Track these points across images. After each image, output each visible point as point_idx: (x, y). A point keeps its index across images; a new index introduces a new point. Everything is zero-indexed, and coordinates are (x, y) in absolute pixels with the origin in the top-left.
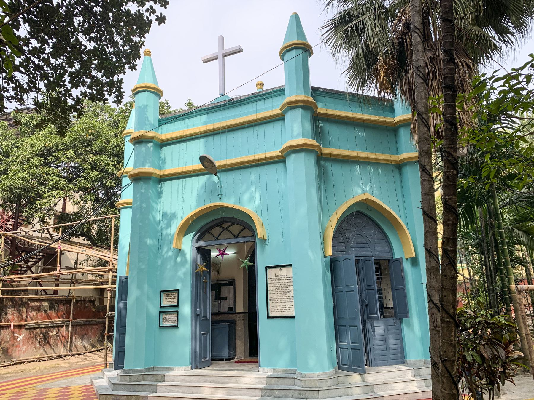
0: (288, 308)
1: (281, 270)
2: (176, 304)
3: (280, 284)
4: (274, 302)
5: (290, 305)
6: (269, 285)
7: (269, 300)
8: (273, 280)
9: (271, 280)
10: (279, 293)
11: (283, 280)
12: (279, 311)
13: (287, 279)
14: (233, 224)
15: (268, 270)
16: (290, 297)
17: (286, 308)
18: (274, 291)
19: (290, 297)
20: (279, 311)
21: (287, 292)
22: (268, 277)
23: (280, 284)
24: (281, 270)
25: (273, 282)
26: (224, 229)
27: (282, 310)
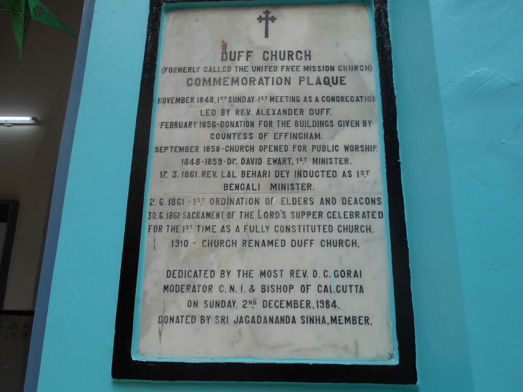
0: (313, 296)
1: (267, 19)
3: (254, 107)
4: (190, 236)
5: (333, 266)
7: (146, 223)
8: (198, 82)
9: (183, 77)
10: (237, 169)
11: (279, 82)
12: (233, 314)
13: (313, 76)
16: (338, 207)
17: (296, 295)
18: (203, 155)
19: (338, 207)
20: (233, 314)
21: (310, 166)
22: (162, 62)
23: (254, 107)
24: (267, 19)
25: (203, 91)
27: (258, 310)
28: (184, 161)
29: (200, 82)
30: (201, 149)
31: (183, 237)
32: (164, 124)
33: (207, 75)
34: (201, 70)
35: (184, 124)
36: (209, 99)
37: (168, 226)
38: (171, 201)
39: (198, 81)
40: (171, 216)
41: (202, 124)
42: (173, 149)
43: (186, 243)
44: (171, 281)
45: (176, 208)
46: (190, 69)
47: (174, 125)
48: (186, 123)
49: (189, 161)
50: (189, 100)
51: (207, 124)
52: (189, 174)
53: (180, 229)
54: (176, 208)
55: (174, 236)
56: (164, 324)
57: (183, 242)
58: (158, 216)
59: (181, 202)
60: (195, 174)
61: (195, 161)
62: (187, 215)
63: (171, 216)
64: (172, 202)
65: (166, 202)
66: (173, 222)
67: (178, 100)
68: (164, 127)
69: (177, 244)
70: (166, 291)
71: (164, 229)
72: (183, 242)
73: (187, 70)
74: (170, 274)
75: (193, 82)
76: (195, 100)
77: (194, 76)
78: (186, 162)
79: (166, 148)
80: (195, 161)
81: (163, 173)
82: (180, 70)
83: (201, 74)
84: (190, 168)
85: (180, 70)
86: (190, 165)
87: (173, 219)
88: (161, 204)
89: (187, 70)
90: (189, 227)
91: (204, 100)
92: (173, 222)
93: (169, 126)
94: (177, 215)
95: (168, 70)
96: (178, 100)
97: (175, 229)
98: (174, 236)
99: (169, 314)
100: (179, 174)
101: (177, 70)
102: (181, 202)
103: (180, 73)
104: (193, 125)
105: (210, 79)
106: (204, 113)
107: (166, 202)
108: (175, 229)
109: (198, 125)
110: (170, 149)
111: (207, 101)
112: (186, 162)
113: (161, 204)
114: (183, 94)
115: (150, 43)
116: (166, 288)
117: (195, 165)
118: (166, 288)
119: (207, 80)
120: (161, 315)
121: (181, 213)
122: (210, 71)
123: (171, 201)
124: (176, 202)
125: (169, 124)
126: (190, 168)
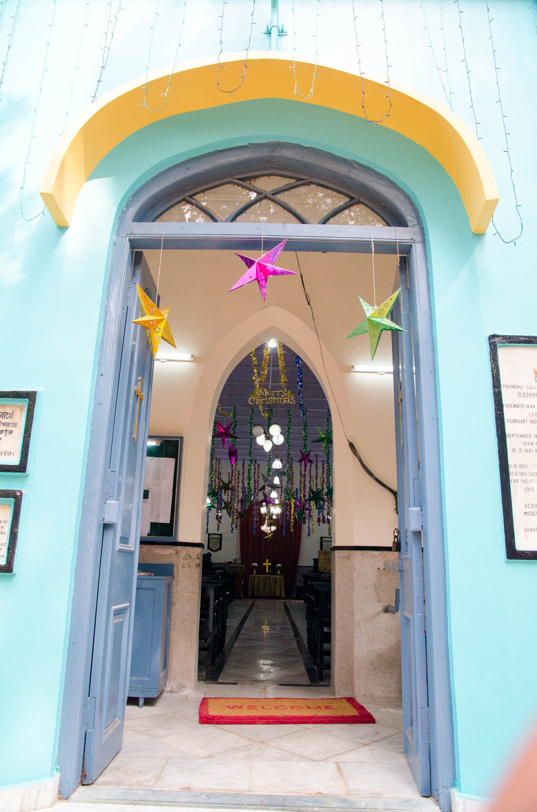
2: (15, 461)
6: (508, 414)
14: (301, 182)
15: (503, 353)
26: (262, 197)
28: (524, 443)
29: (525, 395)
30: (533, 436)
31: (530, 486)
32: (509, 420)
33: (529, 391)
34: (525, 387)
35: (520, 421)
36: (532, 406)
37: (521, 480)
38: (521, 466)
39: (524, 394)
40: (522, 474)
41: (531, 421)
42: (517, 435)
43: (533, 489)
44: (527, 510)
45: (524, 470)
46: (518, 387)
47: (515, 421)
48: (522, 421)
49: (527, 443)
50: (521, 406)
51: (533, 422)
52: (528, 451)
53: (528, 481)
54: (524, 470)
55: (526, 485)
56: (528, 532)
57: (531, 488)
58: (515, 474)
59: (526, 466)
60: (531, 451)
61: (530, 443)
62: (531, 474)
63: (522, 474)
64: (521, 466)
65: (518, 466)
66: (524, 478)
67: (515, 406)
68: (509, 422)
69: (528, 490)
70: (526, 515)
71: (520, 481)
72: (531, 488)
73: (516, 387)
74: (526, 506)
75: (522, 395)
76: (525, 406)
77: (522, 391)
78: (525, 444)
79: (513, 435)
80: (530, 443)
81: (514, 450)
82: (512, 387)
83: (525, 390)
84: (528, 447)
85: (512, 387)
86: (528, 445)
87: (523, 476)
88: (516, 467)
89: (516, 387)
90: (533, 480)
91: (529, 406)
92: (524, 478)
93: (512, 422)
94: (525, 473)
95: (505, 386)
96: (515, 406)
97: (525, 481)
98: (526, 485)
99: (529, 527)
100: (522, 450)
101: (511, 387)
102: (526, 466)
103: (513, 388)
104: (526, 421)
105: (531, 394)
106: (531, 415)
107: (518, 466)
108: (525, 481)
109: (528, 421)
110: (515, 435)
111: (532, 407)
112: (525, 444)
113: (516, 467)
114: (516, 403)
115: (494, 369)
116: (525, 513)
117: (531, 445)
118: (525, 513)
119: (529, 394)
120: (525, 527)
121: (528, 473)
122: (530, 388)
123: (521, 466)
124: (523, 466)
125: (512, 421)
126: (528, 447)
